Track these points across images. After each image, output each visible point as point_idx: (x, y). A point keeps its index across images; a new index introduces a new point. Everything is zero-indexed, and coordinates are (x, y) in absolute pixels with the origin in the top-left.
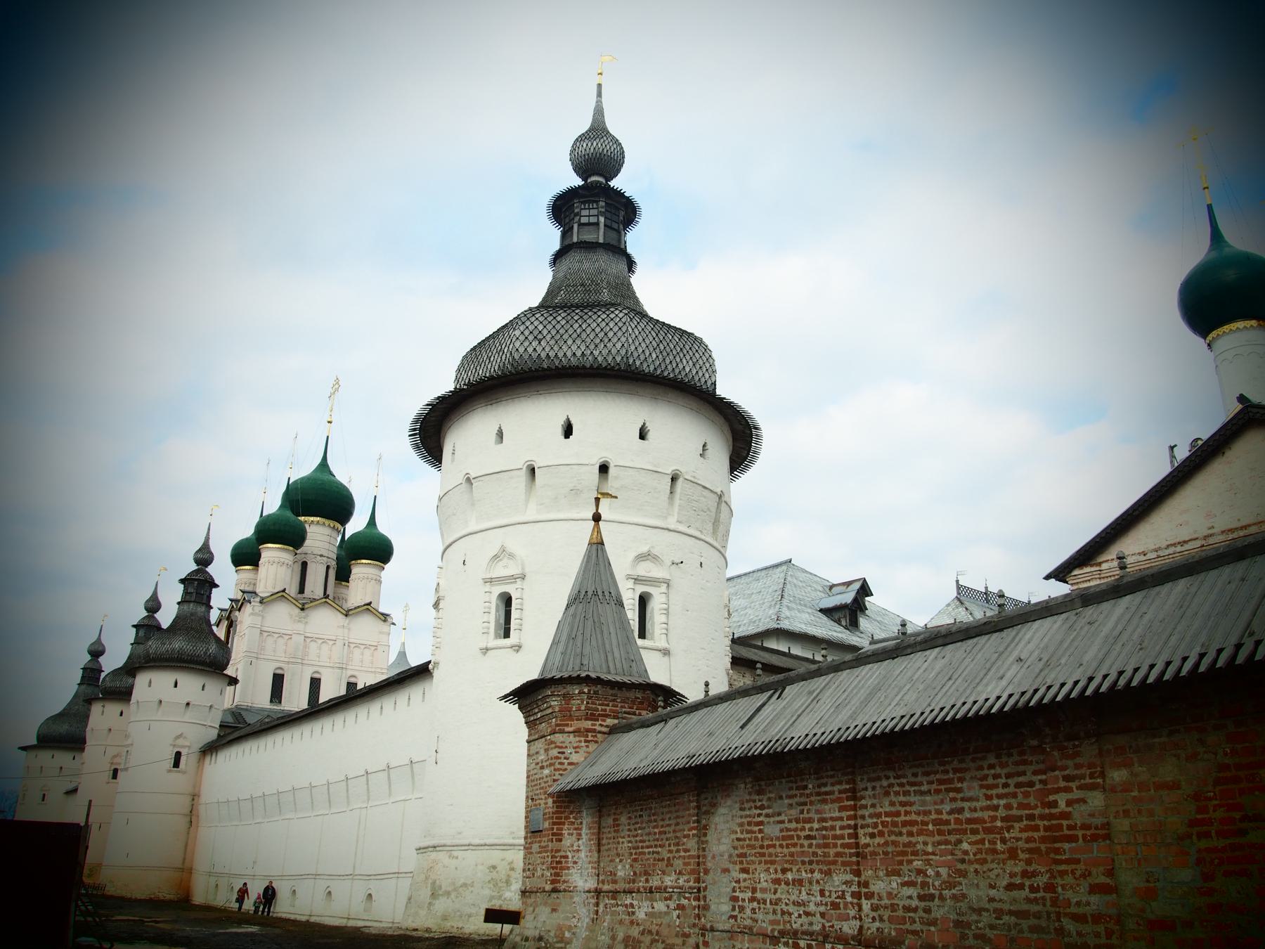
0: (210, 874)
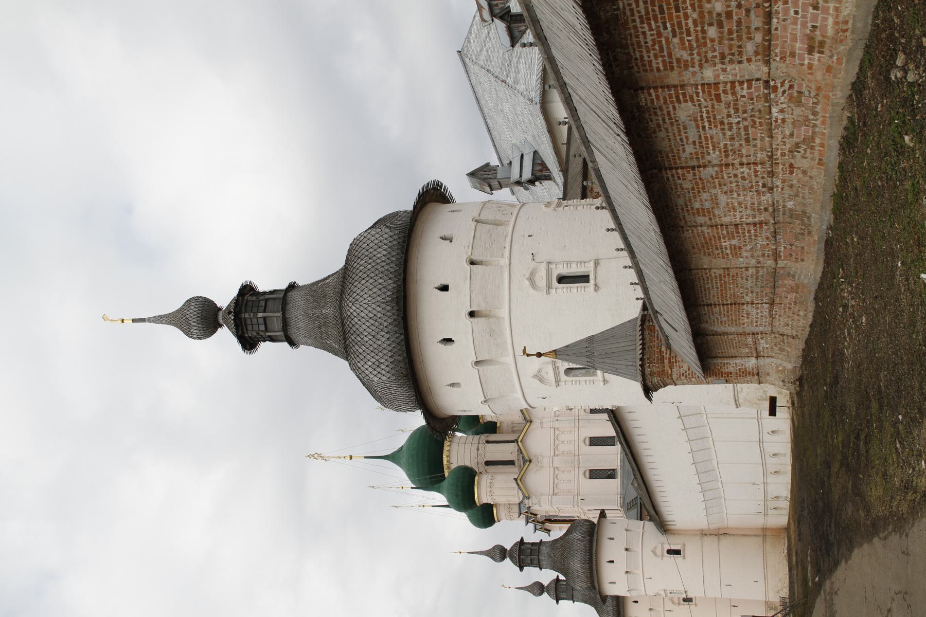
0: (766, 515)
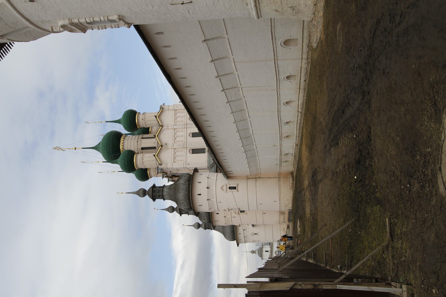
0: (280, 165)
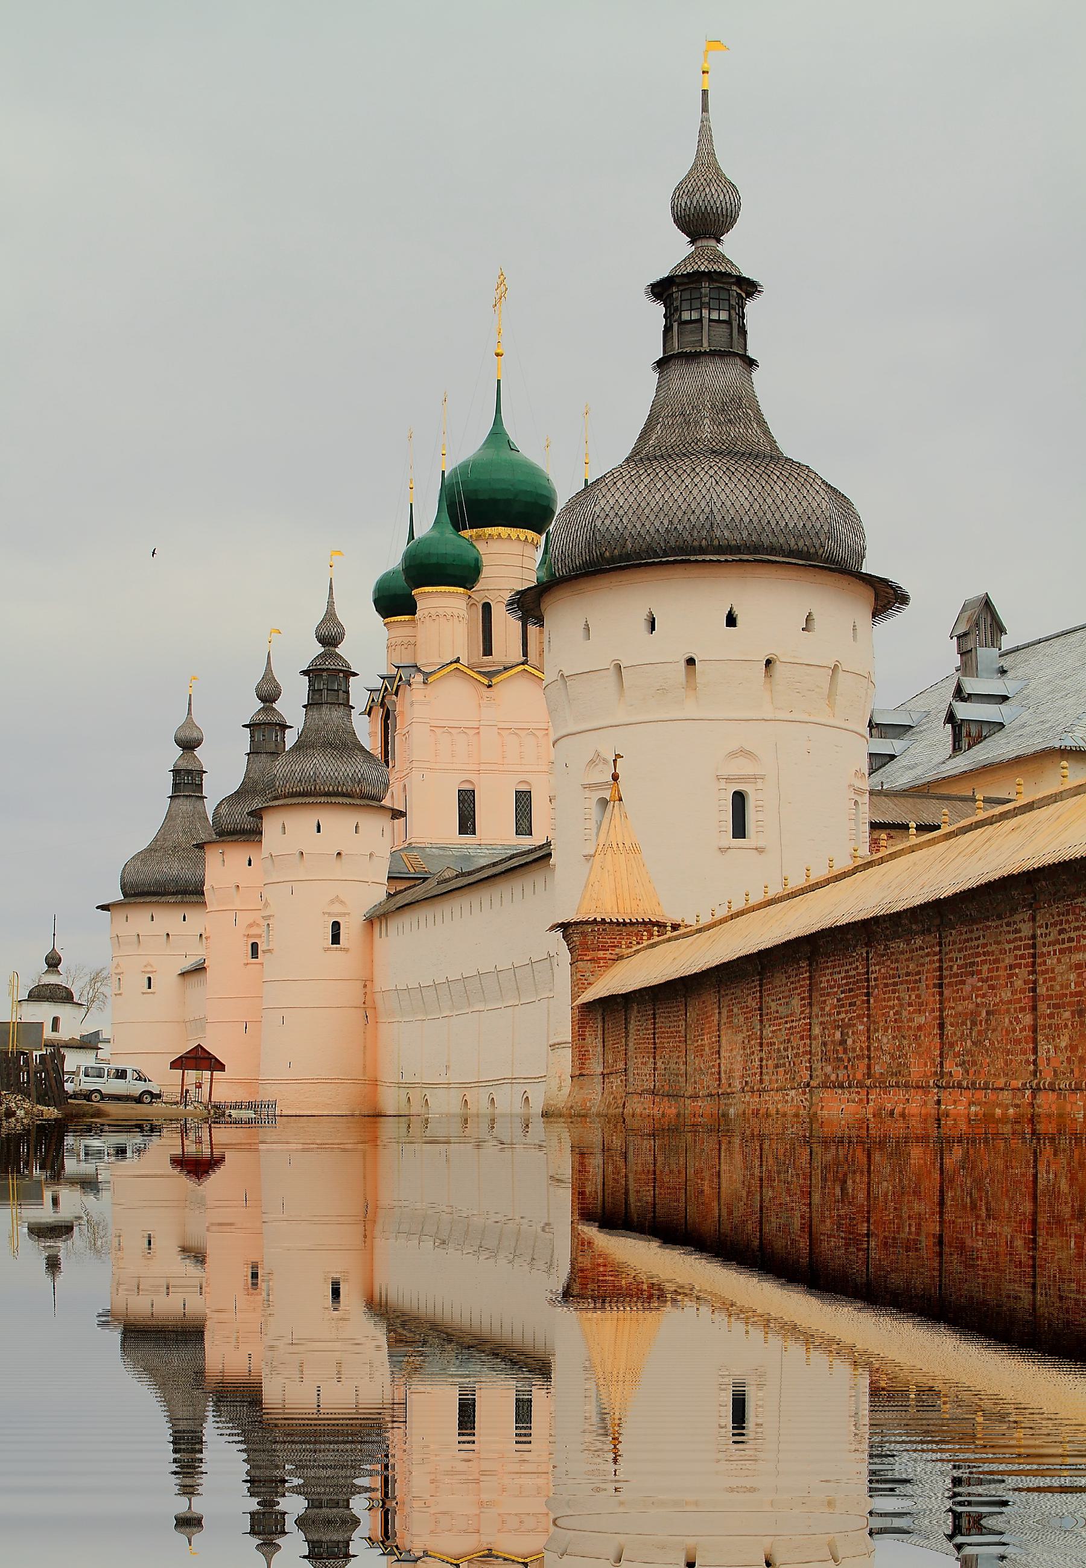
0: (399, 1085)
